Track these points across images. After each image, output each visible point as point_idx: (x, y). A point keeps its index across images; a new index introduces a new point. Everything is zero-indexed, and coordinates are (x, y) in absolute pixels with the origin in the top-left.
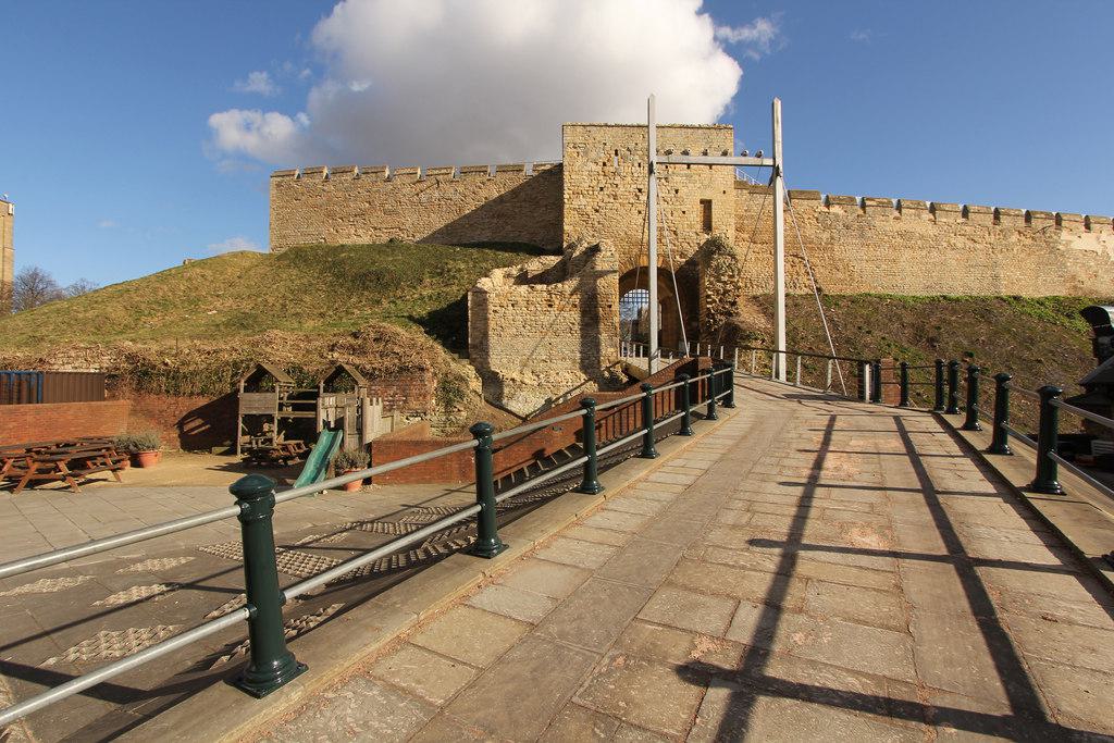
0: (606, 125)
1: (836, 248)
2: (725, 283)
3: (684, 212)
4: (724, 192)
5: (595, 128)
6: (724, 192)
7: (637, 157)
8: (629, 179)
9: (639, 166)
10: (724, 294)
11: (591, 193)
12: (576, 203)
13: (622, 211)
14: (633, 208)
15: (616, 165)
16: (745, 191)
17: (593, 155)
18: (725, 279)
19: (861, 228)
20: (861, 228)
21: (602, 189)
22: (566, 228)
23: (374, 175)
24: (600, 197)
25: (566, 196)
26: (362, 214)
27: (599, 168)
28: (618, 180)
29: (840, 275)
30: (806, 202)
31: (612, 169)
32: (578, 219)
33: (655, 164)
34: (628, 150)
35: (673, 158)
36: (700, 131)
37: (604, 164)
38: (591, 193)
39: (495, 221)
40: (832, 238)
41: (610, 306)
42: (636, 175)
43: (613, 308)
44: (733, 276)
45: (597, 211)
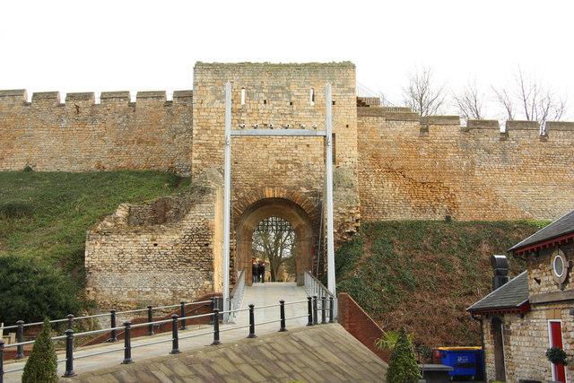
3: (308, 146)
4: (347, 126)
6: (347, 126)
12: (204, 138)
15: (243, 103)
16: (381, 118)
22: (194, 161)
25: (195, 132)
30: (444, 128)
40: (473, 163)
41: (207, 245)
42: (261, 111)
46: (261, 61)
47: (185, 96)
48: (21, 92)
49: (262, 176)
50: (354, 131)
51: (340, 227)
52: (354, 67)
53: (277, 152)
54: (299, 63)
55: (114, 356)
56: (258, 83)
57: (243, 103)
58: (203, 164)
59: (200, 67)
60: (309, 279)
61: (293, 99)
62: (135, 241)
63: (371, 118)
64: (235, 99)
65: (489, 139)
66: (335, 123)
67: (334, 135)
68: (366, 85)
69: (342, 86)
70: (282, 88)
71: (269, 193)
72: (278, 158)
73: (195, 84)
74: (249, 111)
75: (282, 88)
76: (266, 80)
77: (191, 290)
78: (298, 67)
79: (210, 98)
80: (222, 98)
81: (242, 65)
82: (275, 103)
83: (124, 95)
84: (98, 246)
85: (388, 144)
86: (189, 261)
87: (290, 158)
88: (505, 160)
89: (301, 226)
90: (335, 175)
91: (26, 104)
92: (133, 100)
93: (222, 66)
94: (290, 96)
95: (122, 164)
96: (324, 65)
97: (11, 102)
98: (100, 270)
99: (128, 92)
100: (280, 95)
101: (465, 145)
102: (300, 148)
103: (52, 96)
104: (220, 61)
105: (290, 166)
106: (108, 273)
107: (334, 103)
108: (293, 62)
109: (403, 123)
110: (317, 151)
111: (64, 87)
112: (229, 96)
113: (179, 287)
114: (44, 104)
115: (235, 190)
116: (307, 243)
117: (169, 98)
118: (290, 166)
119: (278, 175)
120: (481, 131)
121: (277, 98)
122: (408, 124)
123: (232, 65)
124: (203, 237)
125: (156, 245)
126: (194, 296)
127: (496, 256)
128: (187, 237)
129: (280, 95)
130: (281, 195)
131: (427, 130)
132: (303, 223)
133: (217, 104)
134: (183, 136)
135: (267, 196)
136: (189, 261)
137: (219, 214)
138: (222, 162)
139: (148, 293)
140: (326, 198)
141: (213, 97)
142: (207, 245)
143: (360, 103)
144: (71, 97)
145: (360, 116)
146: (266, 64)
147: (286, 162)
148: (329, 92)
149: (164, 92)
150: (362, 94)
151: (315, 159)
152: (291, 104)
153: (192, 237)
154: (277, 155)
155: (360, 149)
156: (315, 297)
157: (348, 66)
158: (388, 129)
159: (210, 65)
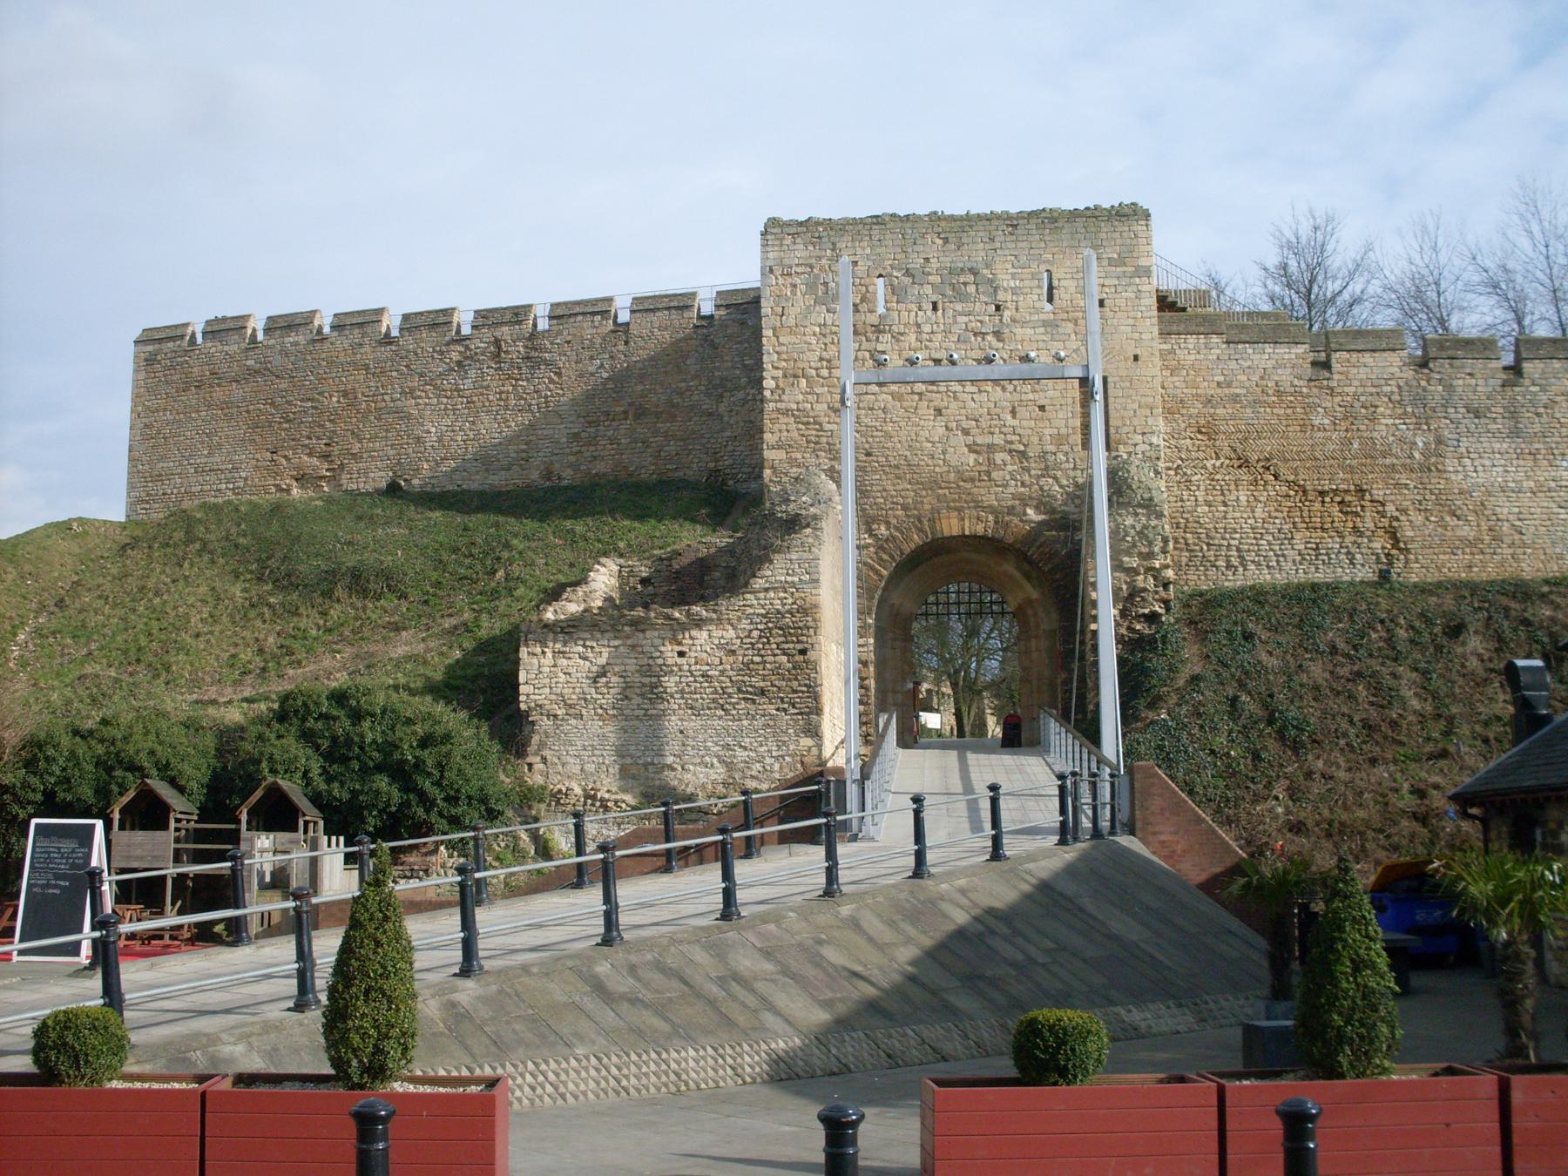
1: (1450, 464)
2: (1135, 571)
3: (1042, 408)
4: (1136, 358)
6: (1136, 358)
7: (928, 289)
8: (913, 337)
9: (935, 308)
10: (1131, 596)
11: (825, 372)
13: (897, 411)
15: (881, 310)
16: (1215, 339)
18: (1134, 562)
19: (1513, 414)
20: (1513, 414)
22: (768, 454)
23: (356, 331)
25: (769, 383)
29: (1467, 532)
30: (1367, 358)
32: (795, 434)
34: (908, 273)
35: (887, 373)
38: (825, 372)
40: (1440, 441)
41: (803, 652)
42: (927, 328)
44: (1150, 556)
46: (923, 210)
47: (743, 309)
49: (934, 483)
50: (1152, 368)
51: (1128, 600)
52: (1147, 215)
53: (965, 424)
54: (1013, 210)
55: (448, 953)
57: (881, 310)
59: (775, 230)
60: (1056, 732)
61: (1001, 296)
62: (633, 647)
63: (1192, 339)
64: (865, 300)
65: (1477, 381)
66: (1107, 353)
67: (1105, 380)
68: (1180, 254)
69: (1120, 262)
71: (951, 526)
73: (768, 271)
76: (932, 249)
77: (768, 760)
78: (1012, 222)
79: (801, 302)
80: (826, 297)
81: (877, 220)
82: (959, 307)
83: (599, 309)
84: (548, 660)
85: (1235, 399)
86: (763, 692)
87: (998, 440)
88: (1515, 433)
89: (1030, 602)
90: (1112, 475)
91: (387, 340)
92: (624, 317)
93: (829, 224)
94: (996, 289)
95: (599, 468)
96: (1074, 215)
98: (555, 716)
99: (609, 300)
101: (1420, 400)
102: (1022, 412)
104: (821, 214)
105: (999, 457)
106: (573, 722)
107: (1101, 303)
108: (998, 209)
109: (1268, 349)
110: (1065, 418)
111: (467, 299)
112: (849, 297)
113: (741, 754)
114: (428, 339)
115: (867, 522)
116: (1044, 644)
117: (707, 308)
118: (999, 457)
119: (972, 480)
120: (1457, 363)
121: (961, 297)
122: (1282, 350)
123: (855, 222)
124: (793, 632)
125: (681, 654)
126: (777, 776)
127: (1520, 663)
128: (755, 634)
130: (980, 529)
131: (1326, 365)
132: (1035, 595)
133: (821, 315)
134: (741, 395)
135: (946, 533)
136: (763, 692)
137: (830, 578)
138: (835, 455)
140: (1091, 535)
143: (1165, 303)
144: (485, 318)
145: (1165, 334)
146: (935, 217)
147: (991, 448)
148: (1084, 272)
150: (1169, 284)
151: (1059, 439)
152: (998, 308)
153: (766, 635)
155: (1169, 412)
156: (1074, 774)
157: (1131, 214)
158: (1233, 365)
159: (801, 224)
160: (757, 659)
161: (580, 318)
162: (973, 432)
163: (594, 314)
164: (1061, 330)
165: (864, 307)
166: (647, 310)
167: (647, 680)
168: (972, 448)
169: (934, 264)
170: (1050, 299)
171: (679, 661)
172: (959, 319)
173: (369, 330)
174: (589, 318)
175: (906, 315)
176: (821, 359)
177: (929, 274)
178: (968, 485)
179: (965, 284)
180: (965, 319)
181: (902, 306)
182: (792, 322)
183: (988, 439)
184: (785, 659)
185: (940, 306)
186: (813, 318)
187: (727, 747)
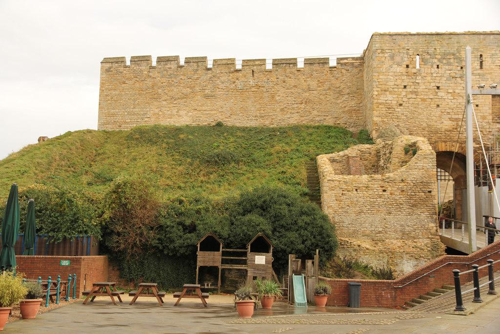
0: (411, 35)
3: (477, 106)
5: (400, 37)
12: (382, 99)
14: (432, 103)
15: (418, 67)
17: (398, 59)
21: (405, 87)
23: (195, 64)
24: (404, 94)
26: (185, 96)
27: (402, 69)
28: (419, 79)
31: (414, 71)
33: (470, 96)
36: (492, 37)
37: (407, 66)
39: (303, 106)
41: (430, 192)
43: (433, 193)
45: (401, 105)
48: (204, 60)
49: (436, 132)
53: (449, 111)
56: (431, 50)
57: (418, 67)
58: (383, 121)
70: (454, 55)
72: (449, 116)
74: (423, 74)
75: (454, 55)
82: (447, 67)
97: (196, 68)
100: (452, 61)
103: (230, 62)
121: (449, 64)
125: (384, 191)
129: (452, 61)
139: (380, 232)
141: (391, 62)
142: (430, 192)
144: (246, 62)
149: (206, 58)
152: (462, 68)
154: (448, 113)
160: (413, 194)
161: (284, 65)
162: (451, 113)
163: (290, 64)
164: (485, 77)
165: (411, 66)
166: (310, 64)
167: (372, 200)
168: (450, 119)
169: (438, 51)
170: (481, 67)
171: (384, 193)
172: (447, 72)
173: (200, 64)
174: (288, 65)
175: (426, 70)
176: (395, 85)
177: (436, 55)
178: (449, 133)
179: (450, 59)
180: (449, 72)
181: (425, 66)
182: (384, 71)
183: (457, 117)
184: (423, 194)
185: (440, 66)
186: (392, 70)
187: (402, 226)
